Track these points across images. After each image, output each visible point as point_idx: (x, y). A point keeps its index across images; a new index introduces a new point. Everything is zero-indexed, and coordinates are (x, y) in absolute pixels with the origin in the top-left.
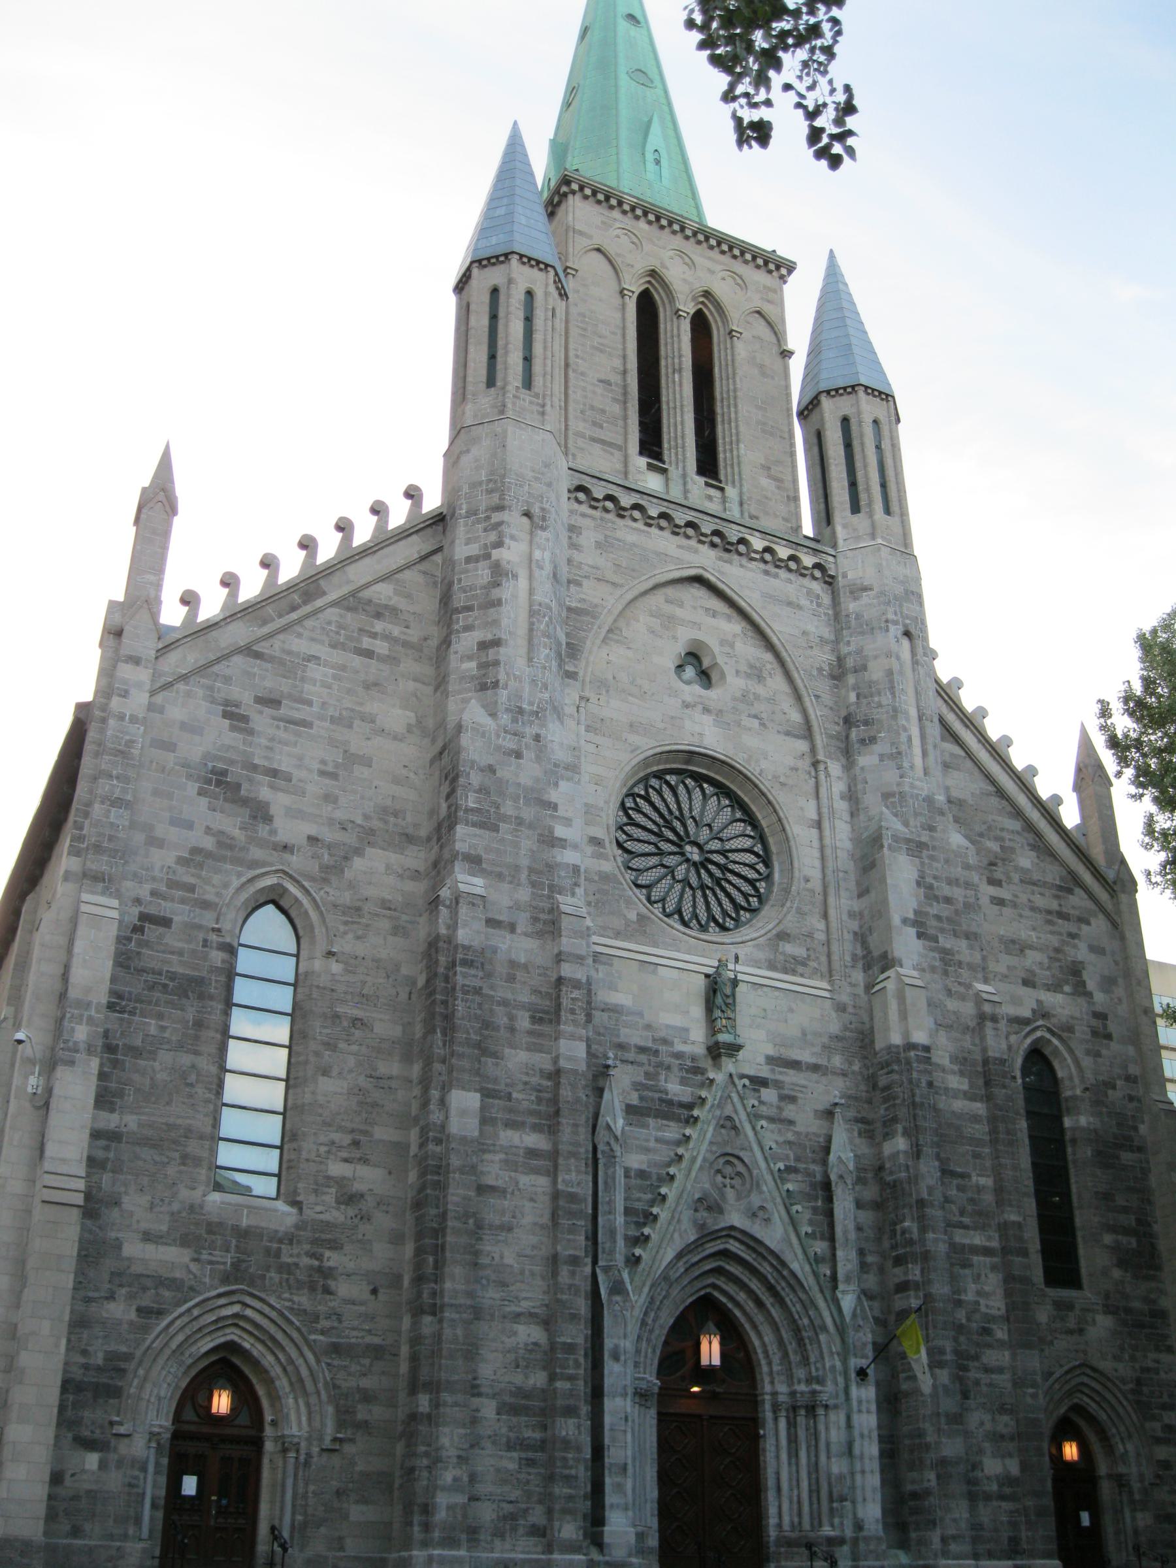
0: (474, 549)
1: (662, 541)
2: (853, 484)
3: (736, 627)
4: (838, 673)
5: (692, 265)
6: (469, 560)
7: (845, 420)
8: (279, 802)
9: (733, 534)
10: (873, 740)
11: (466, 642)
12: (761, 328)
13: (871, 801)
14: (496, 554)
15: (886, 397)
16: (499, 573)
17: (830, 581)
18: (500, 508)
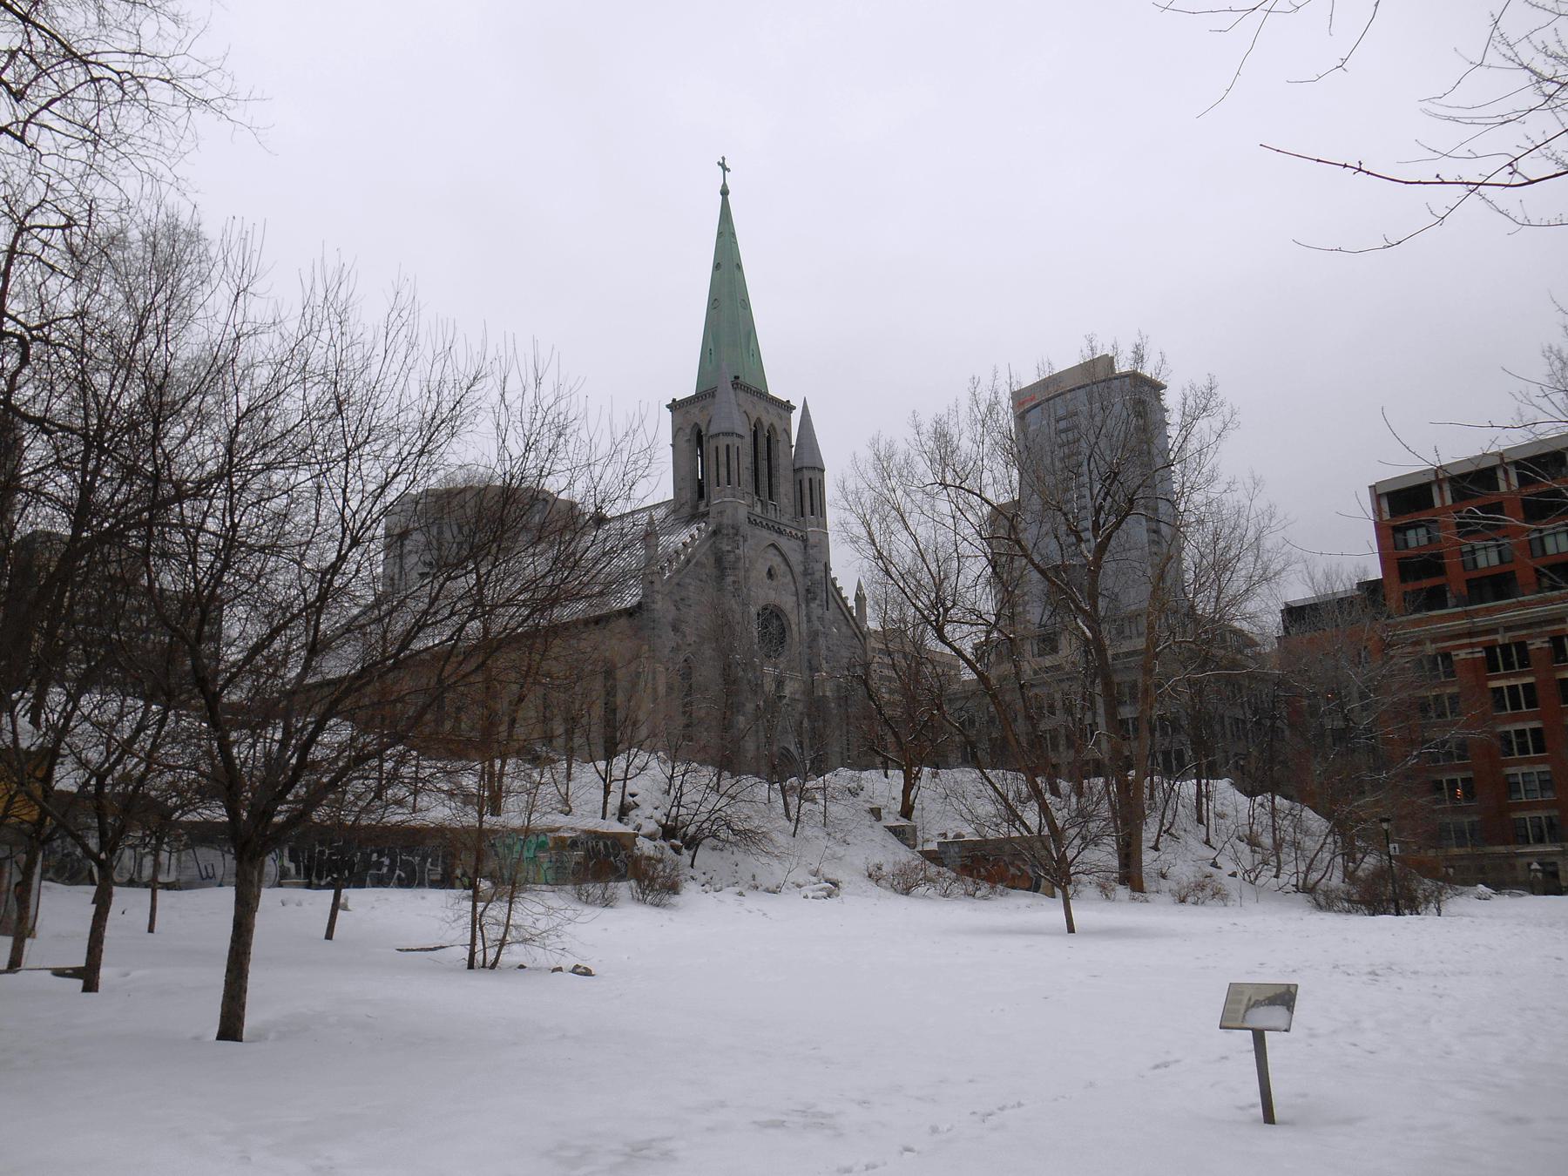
0: (729, 548)
1: (765, 533)
2: (812, 505)
3: (779, 559)
4: (806, 573)
5: (768, 412)
6: (728, 551)
7: (810, 479)
8: (687, 631)
9: (782, 528)
10: (815, 599)
11: (730, 579)
12: (785, 435)
13: (814, 618)
14: (737, 551)
15: (823, 471)
16: (738, 559)
17: (805, 540)
18: (736, 535)
